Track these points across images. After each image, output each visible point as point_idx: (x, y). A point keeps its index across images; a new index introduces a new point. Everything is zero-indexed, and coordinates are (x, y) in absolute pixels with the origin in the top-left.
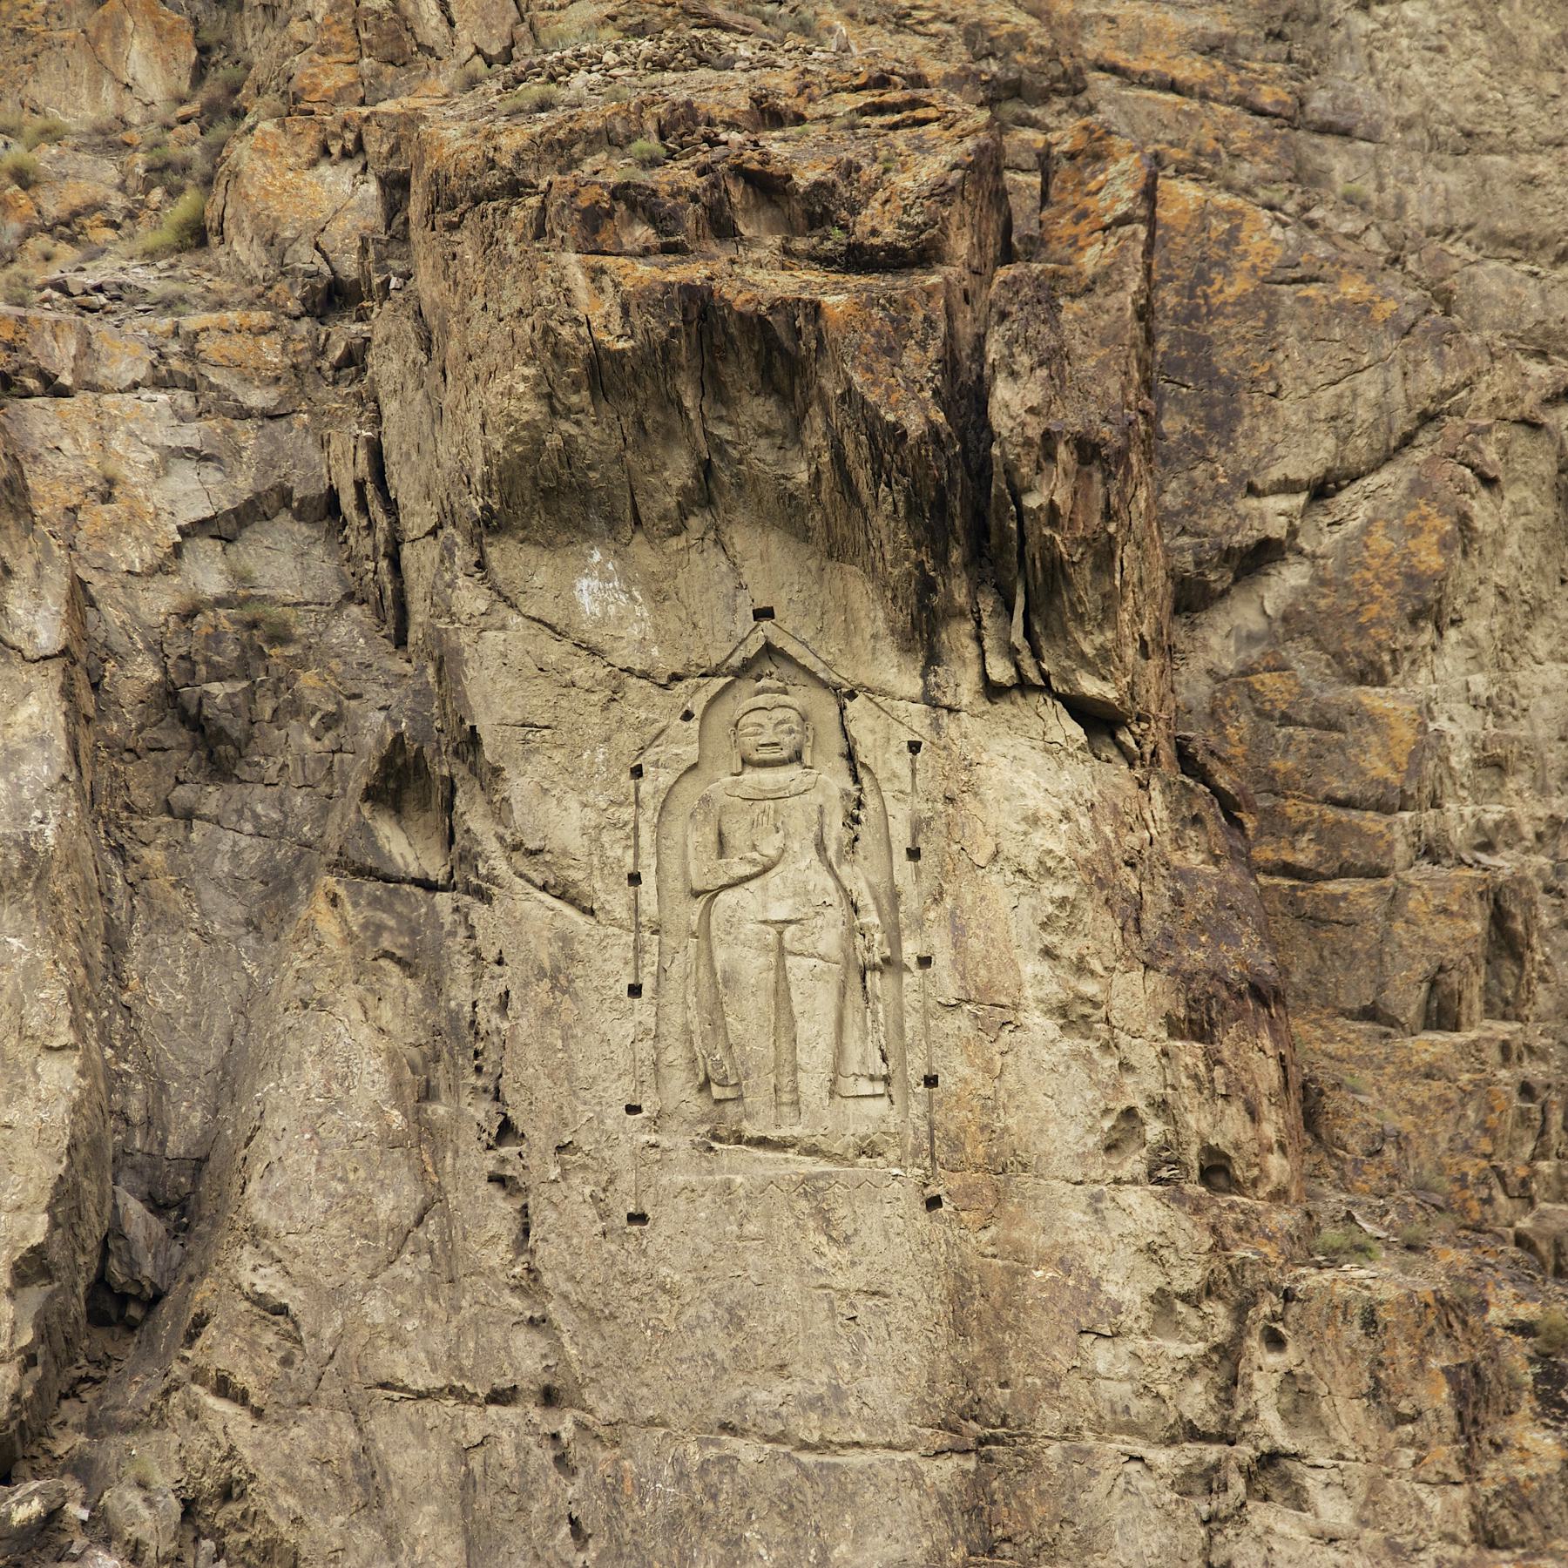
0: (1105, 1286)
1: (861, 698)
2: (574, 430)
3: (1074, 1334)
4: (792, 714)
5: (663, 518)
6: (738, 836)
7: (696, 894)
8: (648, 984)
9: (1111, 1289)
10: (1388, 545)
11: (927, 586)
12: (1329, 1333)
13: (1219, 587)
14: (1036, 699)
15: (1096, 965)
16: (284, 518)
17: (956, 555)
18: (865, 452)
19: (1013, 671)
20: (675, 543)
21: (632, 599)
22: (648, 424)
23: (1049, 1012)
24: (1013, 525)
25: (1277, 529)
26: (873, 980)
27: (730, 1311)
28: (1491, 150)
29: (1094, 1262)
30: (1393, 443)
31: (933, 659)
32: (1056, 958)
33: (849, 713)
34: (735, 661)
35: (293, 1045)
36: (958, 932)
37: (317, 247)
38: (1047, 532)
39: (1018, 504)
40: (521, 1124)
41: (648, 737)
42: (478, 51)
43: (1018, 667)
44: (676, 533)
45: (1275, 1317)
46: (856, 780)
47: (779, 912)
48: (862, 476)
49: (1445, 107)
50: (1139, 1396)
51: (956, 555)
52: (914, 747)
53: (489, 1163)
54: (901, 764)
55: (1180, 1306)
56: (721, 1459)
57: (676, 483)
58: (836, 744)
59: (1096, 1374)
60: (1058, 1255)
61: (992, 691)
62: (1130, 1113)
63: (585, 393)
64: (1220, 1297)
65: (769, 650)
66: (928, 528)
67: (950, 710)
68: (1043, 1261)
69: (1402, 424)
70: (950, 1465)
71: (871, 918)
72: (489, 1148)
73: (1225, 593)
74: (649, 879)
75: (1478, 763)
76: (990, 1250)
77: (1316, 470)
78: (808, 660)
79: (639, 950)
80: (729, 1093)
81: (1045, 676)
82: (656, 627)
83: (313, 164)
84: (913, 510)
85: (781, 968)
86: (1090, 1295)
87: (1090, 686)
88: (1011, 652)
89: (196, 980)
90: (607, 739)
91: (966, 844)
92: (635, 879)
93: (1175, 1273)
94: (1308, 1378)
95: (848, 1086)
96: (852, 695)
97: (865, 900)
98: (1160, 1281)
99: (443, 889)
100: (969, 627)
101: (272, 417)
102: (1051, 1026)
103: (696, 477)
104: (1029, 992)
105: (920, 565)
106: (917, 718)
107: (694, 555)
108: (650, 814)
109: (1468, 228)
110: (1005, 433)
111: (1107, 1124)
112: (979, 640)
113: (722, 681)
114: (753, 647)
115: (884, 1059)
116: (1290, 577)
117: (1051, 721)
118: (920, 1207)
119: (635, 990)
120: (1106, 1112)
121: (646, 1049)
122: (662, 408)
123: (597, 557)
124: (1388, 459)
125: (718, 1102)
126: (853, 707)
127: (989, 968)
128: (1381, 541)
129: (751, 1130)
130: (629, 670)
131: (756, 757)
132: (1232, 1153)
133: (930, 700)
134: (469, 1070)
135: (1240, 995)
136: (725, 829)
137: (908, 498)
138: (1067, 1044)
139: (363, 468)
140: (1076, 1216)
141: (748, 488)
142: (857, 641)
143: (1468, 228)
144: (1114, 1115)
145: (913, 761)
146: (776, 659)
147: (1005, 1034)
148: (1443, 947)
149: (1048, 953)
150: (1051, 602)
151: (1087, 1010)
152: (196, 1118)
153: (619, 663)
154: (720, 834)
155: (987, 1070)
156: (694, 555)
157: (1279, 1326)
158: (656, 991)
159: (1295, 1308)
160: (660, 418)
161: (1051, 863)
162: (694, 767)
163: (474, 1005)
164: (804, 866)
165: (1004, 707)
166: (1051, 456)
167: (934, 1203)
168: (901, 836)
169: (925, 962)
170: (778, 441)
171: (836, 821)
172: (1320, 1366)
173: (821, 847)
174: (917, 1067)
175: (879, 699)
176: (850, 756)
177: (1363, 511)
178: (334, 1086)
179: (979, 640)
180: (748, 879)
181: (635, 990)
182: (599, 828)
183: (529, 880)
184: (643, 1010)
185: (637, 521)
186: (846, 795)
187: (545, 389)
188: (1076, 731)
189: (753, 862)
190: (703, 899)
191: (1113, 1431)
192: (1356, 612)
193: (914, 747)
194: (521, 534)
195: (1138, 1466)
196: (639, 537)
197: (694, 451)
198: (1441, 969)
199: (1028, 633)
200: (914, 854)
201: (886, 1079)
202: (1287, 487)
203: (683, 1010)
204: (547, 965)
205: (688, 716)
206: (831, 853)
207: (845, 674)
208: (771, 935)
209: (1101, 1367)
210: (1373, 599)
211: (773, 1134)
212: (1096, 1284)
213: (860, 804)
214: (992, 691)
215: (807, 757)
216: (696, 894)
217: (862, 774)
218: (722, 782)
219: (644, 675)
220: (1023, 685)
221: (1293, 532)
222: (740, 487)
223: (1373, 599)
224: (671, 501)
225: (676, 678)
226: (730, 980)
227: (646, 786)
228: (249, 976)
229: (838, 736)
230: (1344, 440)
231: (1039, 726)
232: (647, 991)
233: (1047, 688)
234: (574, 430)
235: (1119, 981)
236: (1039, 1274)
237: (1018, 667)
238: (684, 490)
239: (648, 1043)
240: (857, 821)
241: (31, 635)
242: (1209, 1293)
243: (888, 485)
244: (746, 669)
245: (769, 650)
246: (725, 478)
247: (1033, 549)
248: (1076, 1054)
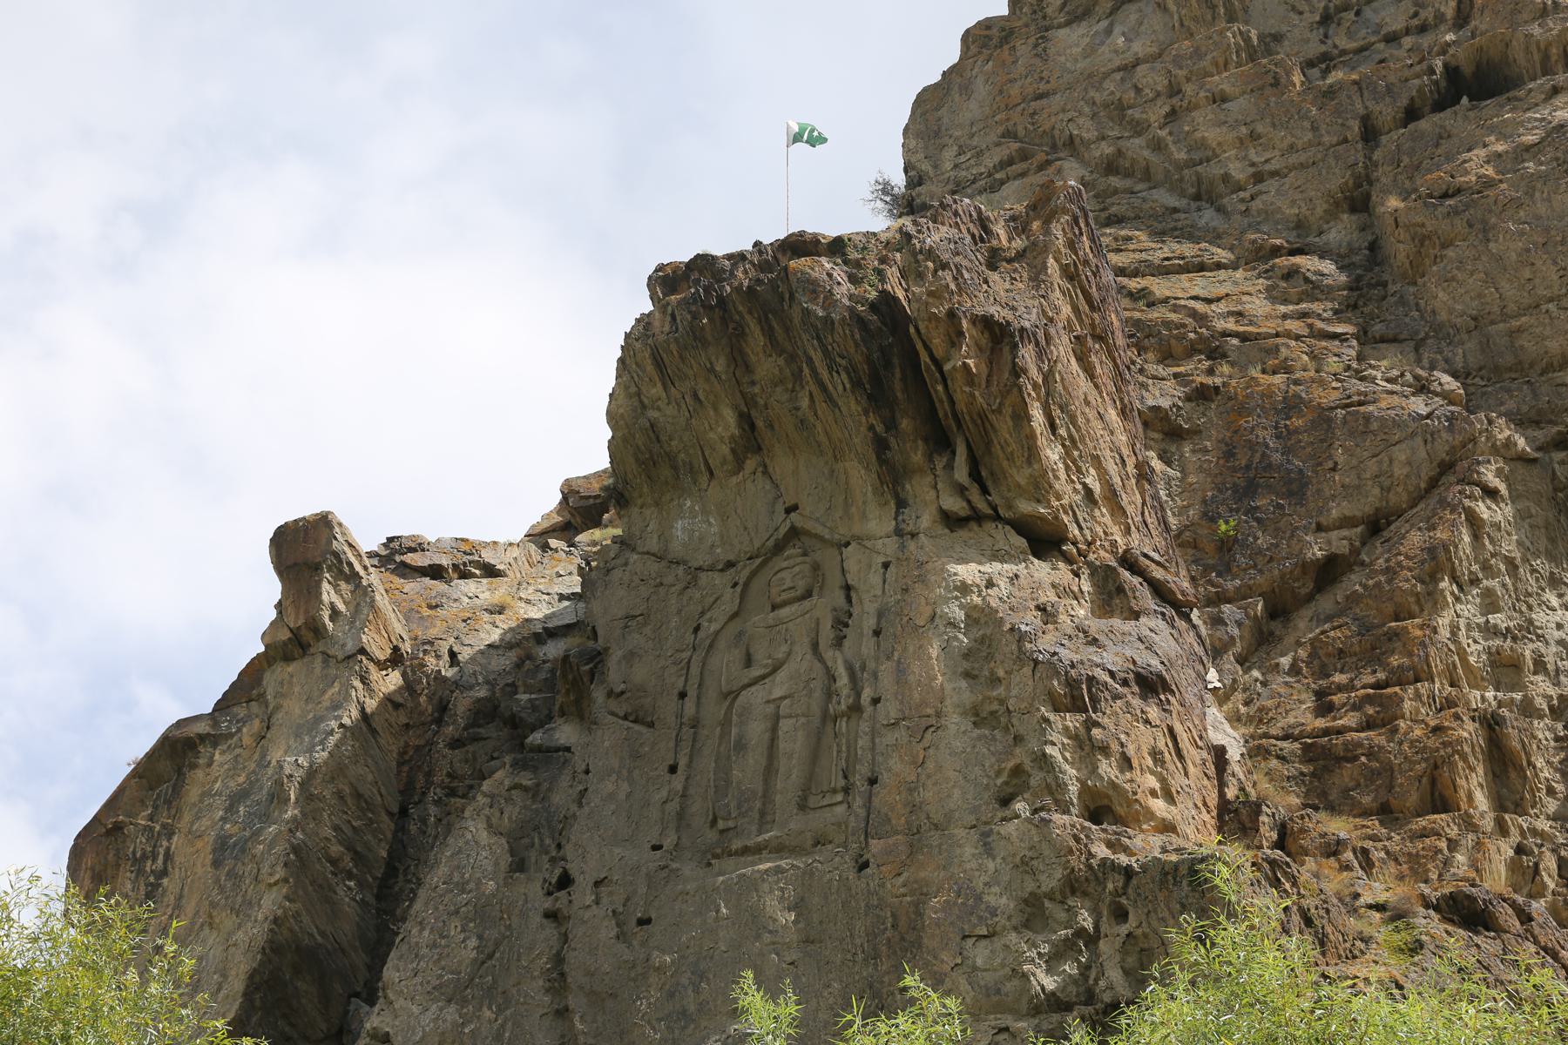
0: (986, 898)
1: (853, 544)
3: (958, 939)
4: (806, 568)
5: (724, 462)
6: (760, 655)
7: (725, 696)
8: (682, 763)
9: (991, 899)
11: (881, 446)
12: (1161, 897)
13: (1304, 591)
14: (990, 526)
15: (1001, 673)
18: (819, 353)
19: (964, 504)
20: (734, 480)
21: (710, 524)
22: (701, 395)
23: (964, 714)
24: (940, 388)
25: (1343, 548)
26: (843, 725)
28: (1493, 323)
30: (1423, 485)
31: (901, 504)
32: (975, 677)
34: (770, 543)
38: (967, 389)
43: (969, 502)
44: (736, 473)
45: (1116, 894)
46: (849, 600)
47: (777, 693)
49: (1459, 307)
50: (1009, 979)
51: (905, 424)
52: (886, 565)
53: (548, 904)
54: (875, 579)
55: (1047, 904)
57: (726, 434)
58: (834, 580)
59: (975, 968)
62: (1017, 771)
63: (659, 385)
64: (1085, 894)
65: (794, 533)
66: (870, 397)
67: (913, 535)
69: (1427, 471)
72: (549, 894)
73: (1310, 598)
74: (692, 693)
75: (1493, 664)
76: (902, 890)
77: (1369, 510)
78: (819, 530)
79: (678, 740)
80: (731, 824)
82: (722, 537)
84: (857, 384)
85: (774, 729)
87: (1025, 507)
88: (961, 490)
90: (679, 612)
91: (912, 614)
92: (682, 695)
93: (1043, 878)
94: (1145, 936)
95: (813, 801)
96: (847, 544)
98: (1030, 886)
100: (930, 478)
102: (967, 724)
103: (740, 426)
104: (948, 702)
105: (871, 428)
106: (890, 546)
107: (749, 484)
108: (701, 653)
109: (1480, 369)
111: (999, 782)
112: (935, 487)
114: (783, 530)
115: (846, 777)
116: (1354, 582)
119: (673, 769)
120: (999, 773)
121: (674, 806)
122: (707, 380)
123: (689, 503)
124: (1421, 498)
125: (722, 832)
129: (736, 845)
130: (700, 569)
131: (778, 600)
132: (1111, 792)
133: (899, 532)
135: (1125, 683)
137: (850, 377)
138: (977, 732)
140: (969, 851)
141: (776, 426)
142: (853, 510)
143: (1480, 369)
144: (1006, 774)
146: (803, 538)
147: (928, 735)
148: (1437, 750)
149: (967, 675)
150: (990, 453)
151: (995, 706)
153: (696, 565)
155: (914, 763)
156: (749, 484)
157: (1124, 901)
158: (689, 766)
159: (1134, 881)
160: (707, 387)
161: (975, 615)
162: (735, 615)
164: (801, 661)
165: (963, 533)
167: (865, 865)
168: (870, 623)
169: (876, 701)
170: (790, 386)
172: (1155, 923)
173: (815, 646)
174: (863, 770)
176: (848, 588)
179: (935, 487)
180: (763, 677)
181: (673, 769)
182: (664, 668)
183: (616, 715)
184: (677, 782)
185: (711, 473)
187: (633, 389)
188: (1022, 542)
189: (766, 666)
190: (729, 699)
191: (987, 1013)
194: (639, 502)
195: (1005, 1036)
197: (735, 407)
198: (1436, 767)
199: (975, 475)
201: (846, 791)
202: (1346, 522)
205: (735, 585)
206: (821, 646)
207: (843, 532)
208: (770, 709)
209: (979, 962)
211: (750, 843)
212: (979, 898)
213: (851, 615)
214: (951, 521)
216: (725, 696)
217: (853, 594)
218: (757, 621)
219: (711, 569)
220: (976, 517)
221: (1355, 552)
222: (771, 427)
224: (725, 450)
226: (741, 746)
227: (701, 634)
231: (989, 541)
233: (997, 518)
235: (1016, 678)
237: (969, 502)
238: (732, 437)
239: (677, 800)
240: (847, 625)
241: (343, 645)
242: (1073, 892)
244: (779, 548)
245: (794, 533)
246: (760, 424)
247: (961, 406)
248: (979, 738)
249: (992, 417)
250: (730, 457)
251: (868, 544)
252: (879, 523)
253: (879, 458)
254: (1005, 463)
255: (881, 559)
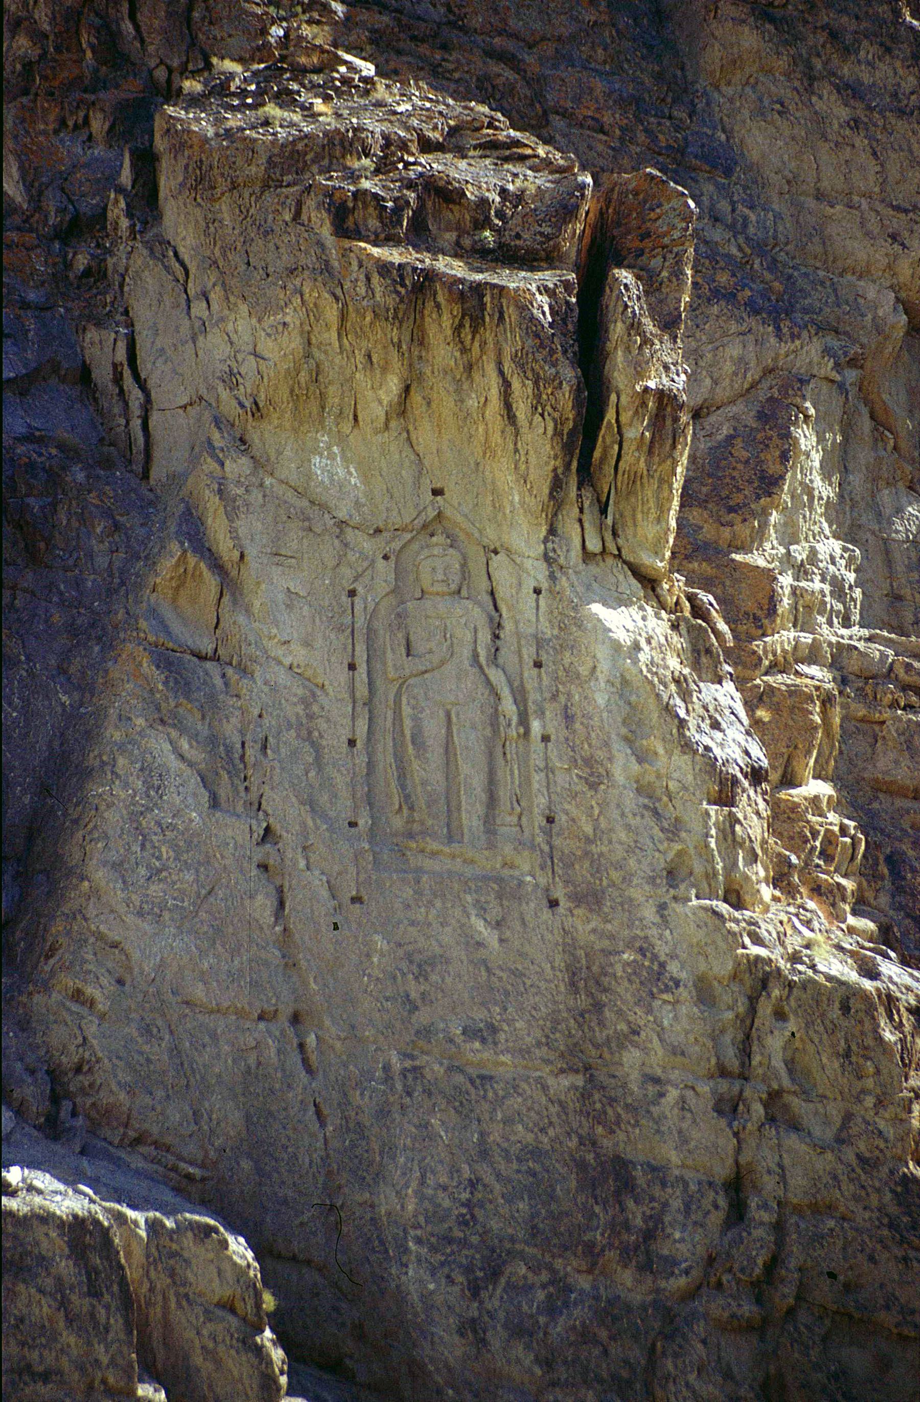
2: (323, 357)
10: (746, 454)
11: (557, 484)
16: (54, 381)
17: (575, 464)
27: (420, 966)
29: (662, 950)
33: (493, 564)
34: (418, 523)
35: (121, 761)
36: (569, 718)
37: (63, 190)
39: (620, 433)
40: (277, 827)
41: (360, 570)
42: (162, 62)
48: (522, 410)
53: (259, 854)
56: (415, 1069)
58: (484, 585)
60: (637, 945)
61: (588, 556)
68: (629, 946)
70: (565, 1081)
71: (509, 707)
74: (362, 669)
81: (619, 549)
83: (56, 132)
84: (557, 433)
86: (659, 974)
89: (26, 702)
96: (496, 552)
97: (506, 693)
99: (211, 659)
101: (42, 309)
105: (555, 470)
110: (621, 387)
113: (408, 536)
117: (621, 578)
118: (545, 902)
126: (496, 560)
127: (590, 745)
128: (740, 451)
134: (241, 789)
136: (412, 638)
139: (121, 355)
141: (434, 405)
145: (537, 601)
152: (27, 799)
154: (408, 640)
163: (243, 744)
165: (593, 569)
166: (644, 404)
169: (545, 739)
171: (485, 636)
175: (515, 557)
177: (725, 431)
178: (152, 793)
179: (580, 521)
181: (352, 743)
186: (491, 619)
192: (728, 497)
193: (537, 591)
196: (356, 431)
200: (538, 665)
203: (385, 758)
204: (293, 720)
207: (491, 535)
210: (739, 490)
212: (662, 965)
215: (464, 593)
223: (739, 490)
224: (380, 412)
225: (378, 531)
226: (418, 740)
228: (63, 704)
229: (485, 577)
230: (716, 382)
232: (359, 744)
234: (323, 357)
236: (625, 956)
240: (497, 637)
243: (542, 415)
249: (645, 480)
250: (382, 418)
251: (518, 560)
252: (525, 537)
253: (551, 493)
254: (639, 516)
255: (533, 584)
